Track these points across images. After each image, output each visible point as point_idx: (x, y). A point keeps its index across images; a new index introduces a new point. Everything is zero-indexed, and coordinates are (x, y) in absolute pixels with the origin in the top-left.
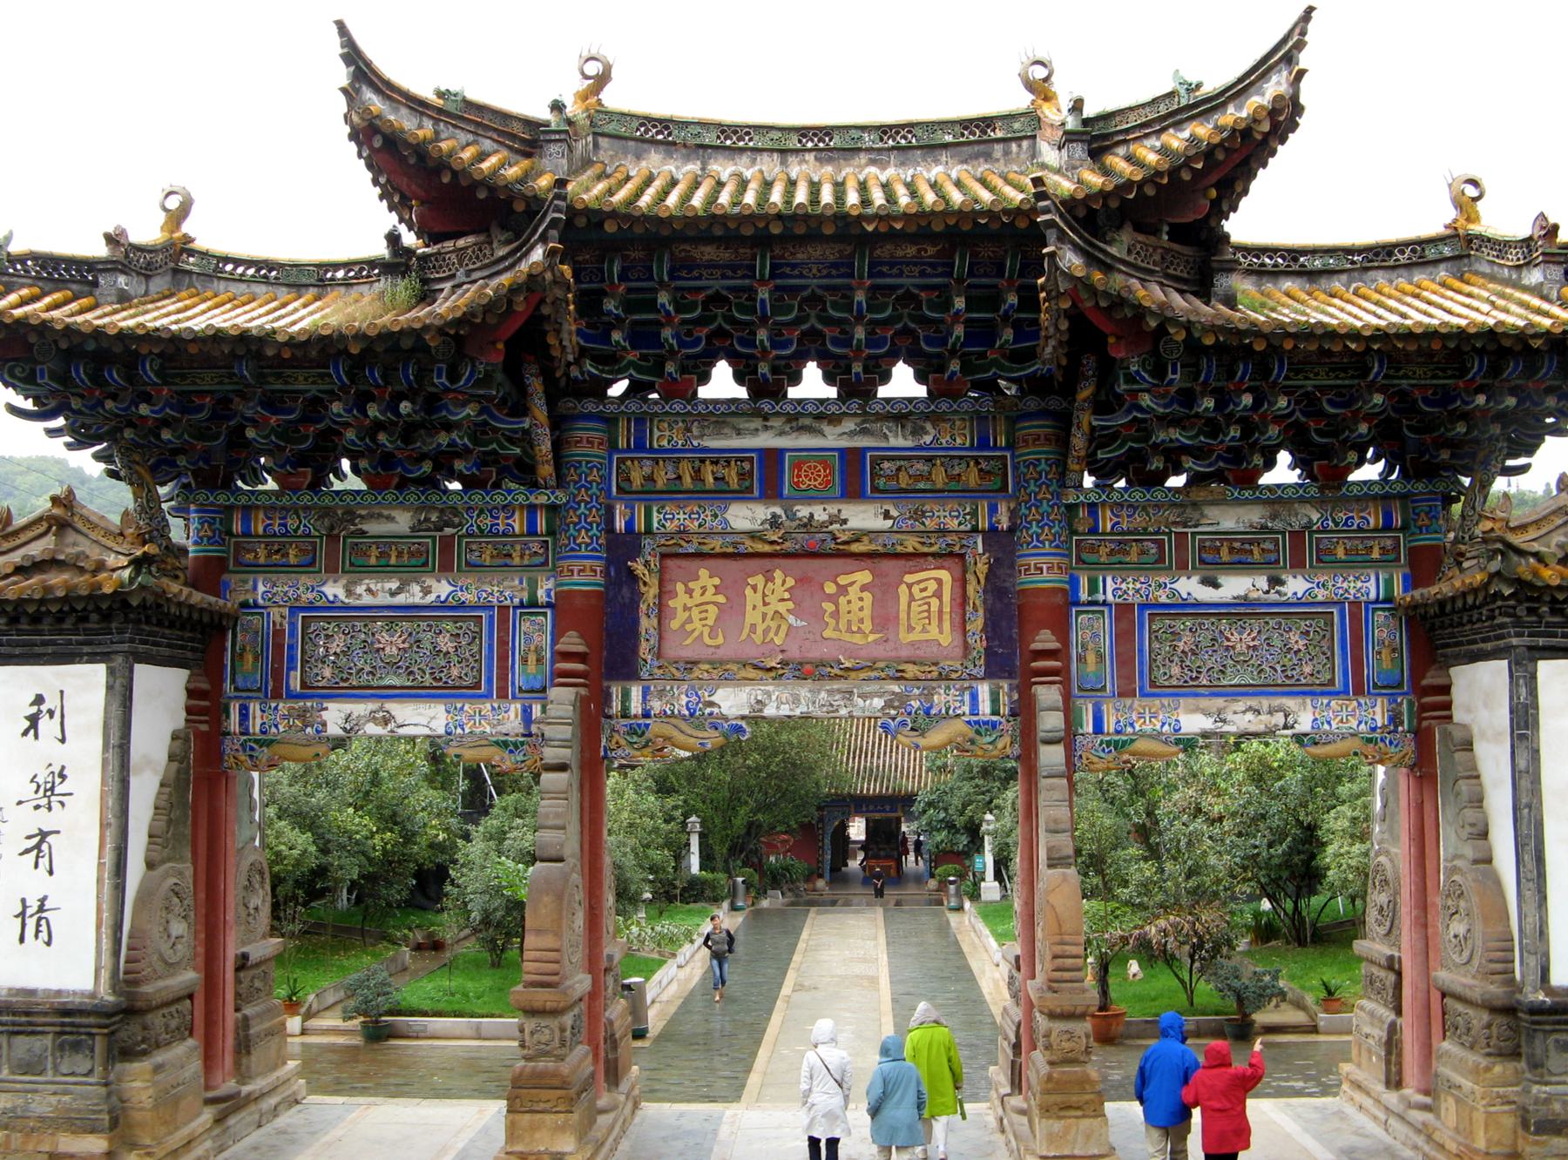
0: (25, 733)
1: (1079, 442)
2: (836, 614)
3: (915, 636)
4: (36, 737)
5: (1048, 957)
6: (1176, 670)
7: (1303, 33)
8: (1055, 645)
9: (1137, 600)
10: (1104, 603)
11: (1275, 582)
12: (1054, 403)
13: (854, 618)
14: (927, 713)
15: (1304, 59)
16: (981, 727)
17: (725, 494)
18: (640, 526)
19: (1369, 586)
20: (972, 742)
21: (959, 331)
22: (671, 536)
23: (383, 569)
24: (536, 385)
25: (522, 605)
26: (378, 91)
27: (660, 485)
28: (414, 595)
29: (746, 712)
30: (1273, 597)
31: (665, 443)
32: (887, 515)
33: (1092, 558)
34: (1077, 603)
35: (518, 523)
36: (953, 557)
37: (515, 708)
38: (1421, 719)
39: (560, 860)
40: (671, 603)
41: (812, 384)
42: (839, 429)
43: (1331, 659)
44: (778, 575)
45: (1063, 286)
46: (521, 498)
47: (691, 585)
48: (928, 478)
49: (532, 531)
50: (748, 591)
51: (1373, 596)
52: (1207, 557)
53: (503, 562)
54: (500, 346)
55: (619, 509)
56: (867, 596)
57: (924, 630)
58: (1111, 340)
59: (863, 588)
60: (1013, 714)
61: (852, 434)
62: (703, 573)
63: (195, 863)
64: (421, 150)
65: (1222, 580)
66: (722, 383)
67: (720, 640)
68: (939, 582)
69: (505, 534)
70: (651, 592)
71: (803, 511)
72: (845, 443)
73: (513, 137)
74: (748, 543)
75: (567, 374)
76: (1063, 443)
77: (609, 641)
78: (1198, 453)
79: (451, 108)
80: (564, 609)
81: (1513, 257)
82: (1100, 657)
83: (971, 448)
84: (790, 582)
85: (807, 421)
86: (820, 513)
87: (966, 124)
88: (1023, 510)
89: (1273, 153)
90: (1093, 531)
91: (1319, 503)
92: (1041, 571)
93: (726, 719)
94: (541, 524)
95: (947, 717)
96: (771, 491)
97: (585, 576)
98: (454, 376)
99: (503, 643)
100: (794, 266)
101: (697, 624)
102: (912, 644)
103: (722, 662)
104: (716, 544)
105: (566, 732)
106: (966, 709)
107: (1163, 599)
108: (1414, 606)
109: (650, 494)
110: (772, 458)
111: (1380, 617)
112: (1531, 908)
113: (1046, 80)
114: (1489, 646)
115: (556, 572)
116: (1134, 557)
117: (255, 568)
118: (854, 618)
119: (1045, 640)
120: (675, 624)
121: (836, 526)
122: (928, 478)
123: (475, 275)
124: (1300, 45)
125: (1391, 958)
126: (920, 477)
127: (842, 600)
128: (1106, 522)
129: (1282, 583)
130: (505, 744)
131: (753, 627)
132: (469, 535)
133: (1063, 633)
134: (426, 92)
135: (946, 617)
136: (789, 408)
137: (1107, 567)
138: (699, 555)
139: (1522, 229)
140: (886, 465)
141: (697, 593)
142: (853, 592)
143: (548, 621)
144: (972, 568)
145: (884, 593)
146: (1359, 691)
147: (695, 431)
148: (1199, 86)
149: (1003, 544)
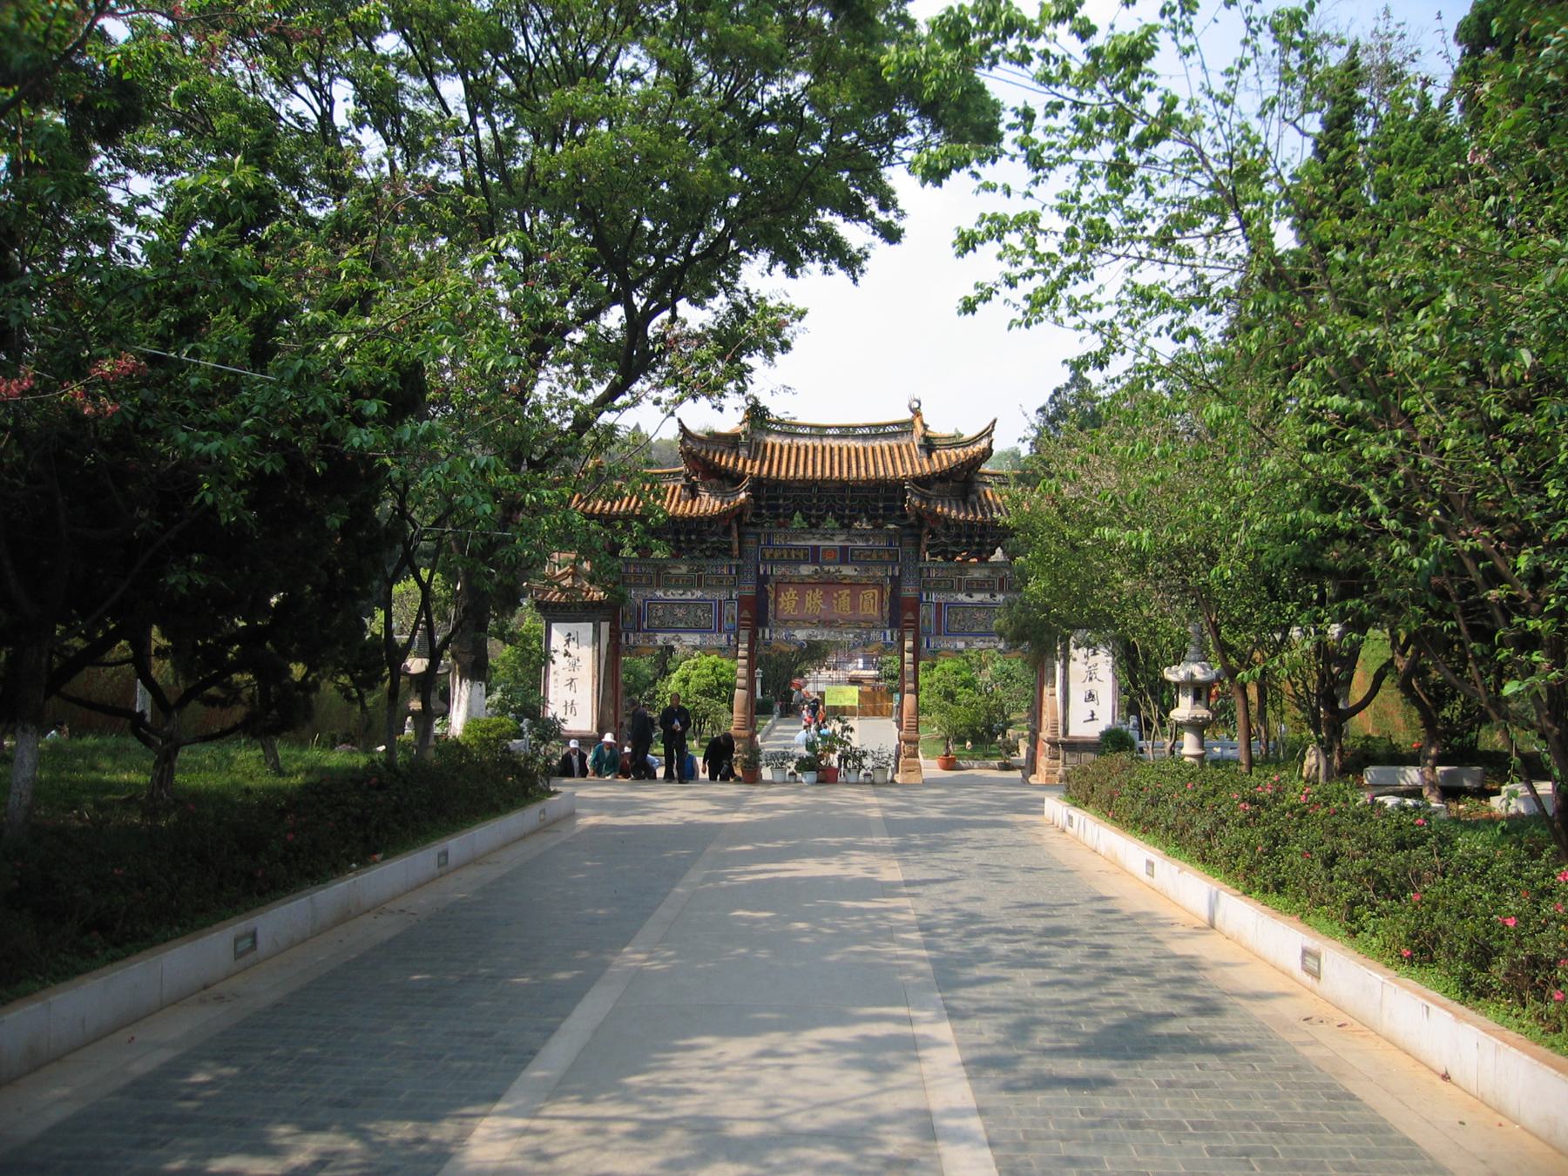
11: (992, 596)
12: (916, 531)
17: (798, 562)
23: (677, 587)
24: (734, 525)
28: (689, 596)
36: (880, 586)
37: (724, 637)
70: (772, 596)
77: (757, 613)
80: (743, 602)
86: (832, 569)
92: (909, 591)
96: (815, 561)
97: (749, 590)
109: (774, 562)
115: (738, 588)
117: (630, 585)
119: (909, 616)
133: (917, 613)
145: (854, 597)
149: (896, 582)
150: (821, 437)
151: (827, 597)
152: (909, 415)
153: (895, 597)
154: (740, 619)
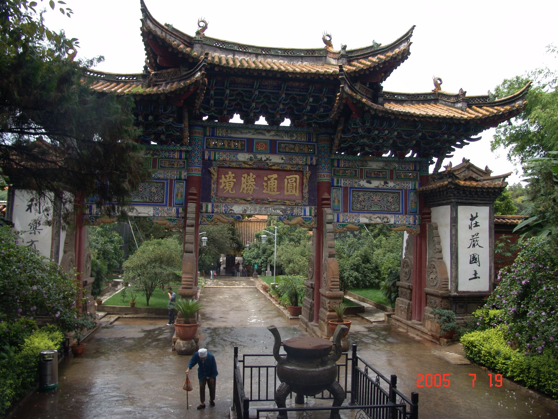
0: (27, 210)
1: (337, 142)
2: (267, 186)
3: (289, 193)
4: (31, 211)
5: (329, 281)
6: (359, 206)
7: (412, 33)
8: (329, 197)
9: (350, 186)
10: (341, 187)
11: (386, 183)
13: (272, 187)
14: (292, 215)
15: (412, 39)
16: (306, 219)
17: (237, 151)
18: (212, 158)
19: (410, 185)
20: (304, 223)
21: (309, 108)
22: (221, 161)
24: (186, 114)
25: (177, 179)
26: (151, 21)
27: (218, 147)
29: (241, 212)
30: (385, 187)
31: (220, 135)
32: (282, 159)
33: (338, 174)
34: (333, 186)
35: (176, 155)
36: (300, 172)
37: (174, 209)
38: (422, 221)
39: (191, 252)
40: (220, 181)
41: (262, 121)
42: (270, 134)
43: (399, 205)
44: (251, 174)
45: (345, 96)
46: (178, 148)
47: (226, 176)
48: (294, 149)
49: (181, 158)
51: (411, 188)
52: (369, 175)
53: (172, 167)
54: (182, 101)
55: (206, 153)
56: (276, 181)
57: (291, 192)
58: (354, 113)
59: (275, 179)
60: (315, 216)
61: (273, 135)
62: (230, 173)
63: (75, 253)
64: (163, 41)
65: (372, 182)
66: (236, 119)
67: (234, 192)
68: (296, 178)
69: (172, 158)
71: (259, 156)
72: (271, 138)
73: (185, 41)
74: (243, 165)
75: (195, 113)
76: (332, 141)
78: (370, 146)
79: (170, 30)
80: (189, 181)
81: (452, 100)
82: (339, 201)
83: (306, 142)
84: (255, 176)
85: (261, 131)
87: (308, 51)
88: (320, 160)
89: (399, 65)
90: (338, 166)
91: (398, 162)
92: (324, 177)
93: (235, 214)
94: (184, 155)
95: (297, 216)
96: (250, 151)
98: (165, 110)
99: (171, 190)
100: (264, 86)
101: (228, 187)
102: (288, 195)
103: (235, 198)
104: (234, 165)
105: (194, 216)
106: (303, 214)
107: (356, 186)
108: (423, 191)
109: (215, 149)
110: (250, 141)
111: (412, 194)
112: (453, 270)
113: (330, 40)
114: (445, 202)
115: (188, 170)
116: (349, 174)
118: (272, 187)
119: (326, 196)
120: (221, 187)
121: (268, 161)
122: (294, 149)
123: (173, 80)
124: (411, 36)
125: (409, 286)
126: (291, 149)
128: (342, 164)
129: (387, 183)
130: (171, 220)
131: (244, 189)
132: (162, 158)
133: (329, 193)
134: (163, 24)
135: (298, 188)
136: (256, 127)
137: (342, 177)
138: (229, 168)
139: (456, 92)
140: (282, 145)
141: (228, 178)
143: (184, 184)
144: (305, 175)
145: (280, 180)
146: (406, 214)
147: (229, 132)
148: (380, 44)
149: (314, 168)
150: (257, 55)
151: (258, 179)
152: (323, 46)
153: (312, 179)
154: (187, 194)
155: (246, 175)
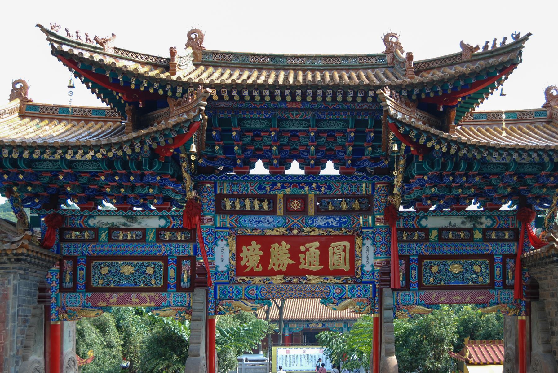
2: (305, 259)
41: (295, 169)
44: (284, 243)
47: (249, 247)
50: (272, 249)
62: (254, 243)
66: (259, 169)
68: (345, 246)
127: (307, 253)
131: (274, 265)
142: (312, 250)
155: (277, 244)
